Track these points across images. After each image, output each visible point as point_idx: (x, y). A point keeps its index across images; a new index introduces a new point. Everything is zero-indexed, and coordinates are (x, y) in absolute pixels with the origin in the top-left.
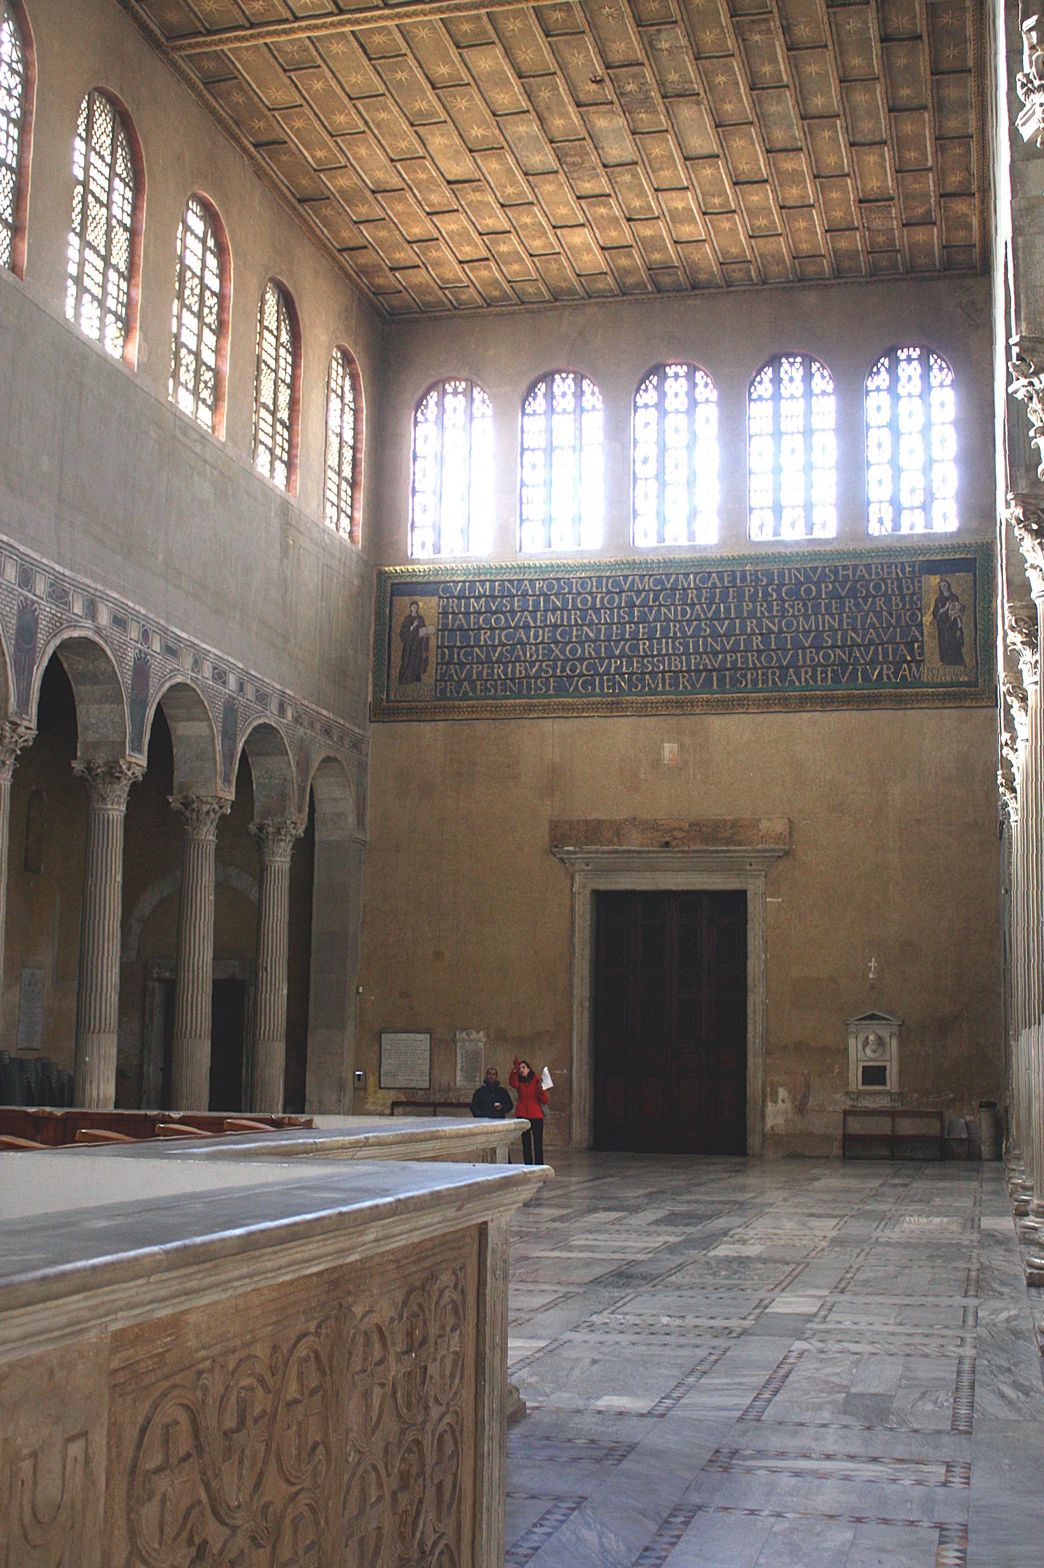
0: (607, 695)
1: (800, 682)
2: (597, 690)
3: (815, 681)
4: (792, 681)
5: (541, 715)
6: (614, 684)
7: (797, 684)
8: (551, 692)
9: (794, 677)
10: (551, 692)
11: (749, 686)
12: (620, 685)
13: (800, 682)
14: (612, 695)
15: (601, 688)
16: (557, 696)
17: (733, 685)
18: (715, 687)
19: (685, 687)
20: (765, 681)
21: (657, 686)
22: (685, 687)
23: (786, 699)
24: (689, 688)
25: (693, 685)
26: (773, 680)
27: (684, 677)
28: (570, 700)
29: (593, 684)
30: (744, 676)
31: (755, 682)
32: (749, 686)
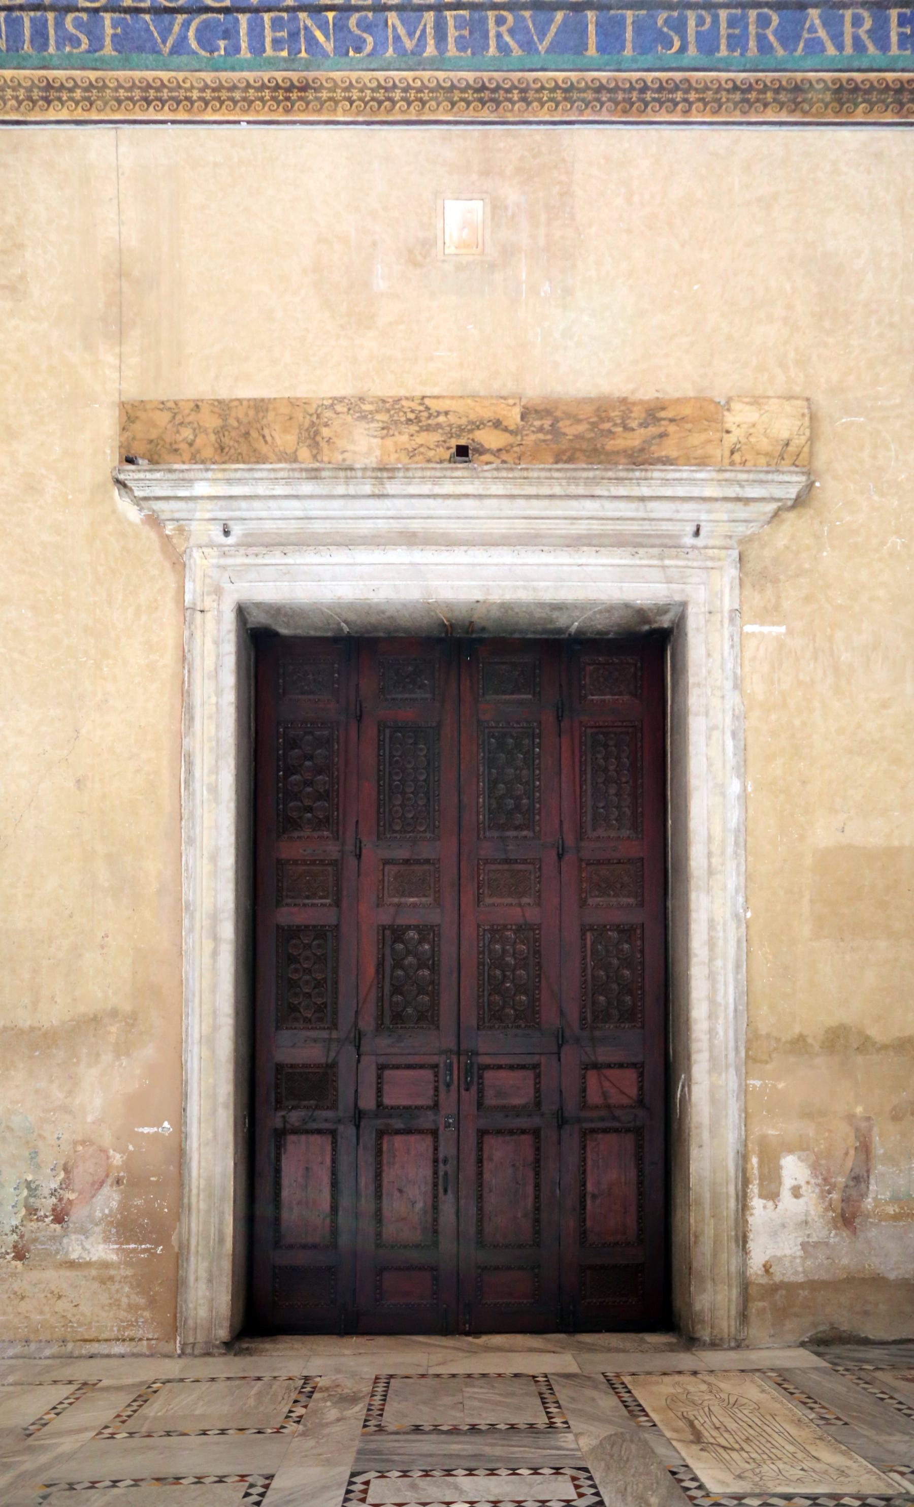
0: (272, 64)
1: (840, 47)
2: (245, 53)
3: (883, 44)
4: (815, 46)
5: (79, 115)
6: (294, 36)
7: (831, 50)
8: (108, 50)
9: (822, 33)
10: (108, 50)
11: (692, 51)
12: (312, 41)
13: (840, 47)
14: (290, 63)
15: (257, 48)
16: (126, 65)
17: (642, 49)
18: (592, 51)
19: (504, 49)
20: (737, 42)
21: (421, 42)
22: (504, 49)
23: (797, 88)
24: (517, 52)
25: (528, 46)
26: (761, 39)
27: (500, 21)
28: (165, 75)
29: (230, 34)
30: (680, 27)
31: (708, 44)
32: (692, 51)
